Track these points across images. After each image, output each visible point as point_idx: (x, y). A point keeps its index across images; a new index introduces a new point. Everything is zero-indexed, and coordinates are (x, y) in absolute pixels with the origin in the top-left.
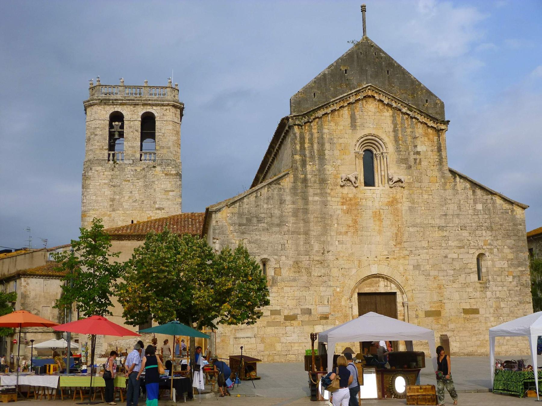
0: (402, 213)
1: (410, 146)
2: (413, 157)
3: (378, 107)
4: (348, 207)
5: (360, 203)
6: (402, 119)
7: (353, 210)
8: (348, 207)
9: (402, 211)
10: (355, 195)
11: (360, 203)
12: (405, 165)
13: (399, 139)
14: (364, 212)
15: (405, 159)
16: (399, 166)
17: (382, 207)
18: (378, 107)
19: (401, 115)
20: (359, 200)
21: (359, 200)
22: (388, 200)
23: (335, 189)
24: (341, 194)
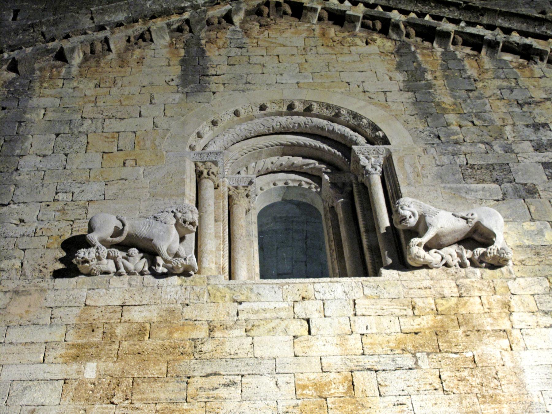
0: (521, 385)
1: (508, 128)
2: (537, 159)
3: (323, 35)
4: (113, 367)
5: (208, 347)
6: (448, 56)
7: (155, 379)
8: (113, 367)
9: (518, 372)
10: (171, 312)
11: (208, 347)
12: (495, 186)
13: (444, 109)
14: (235, 392)
15: (491, 167)
16: (458, 190)
17: (368, 361)
18: (323, 35)
19: (438, 50)
20: (202, 333)
21: (202, 333)
22: (410, 324)
23: (43, 290)
24: (76, 311)
